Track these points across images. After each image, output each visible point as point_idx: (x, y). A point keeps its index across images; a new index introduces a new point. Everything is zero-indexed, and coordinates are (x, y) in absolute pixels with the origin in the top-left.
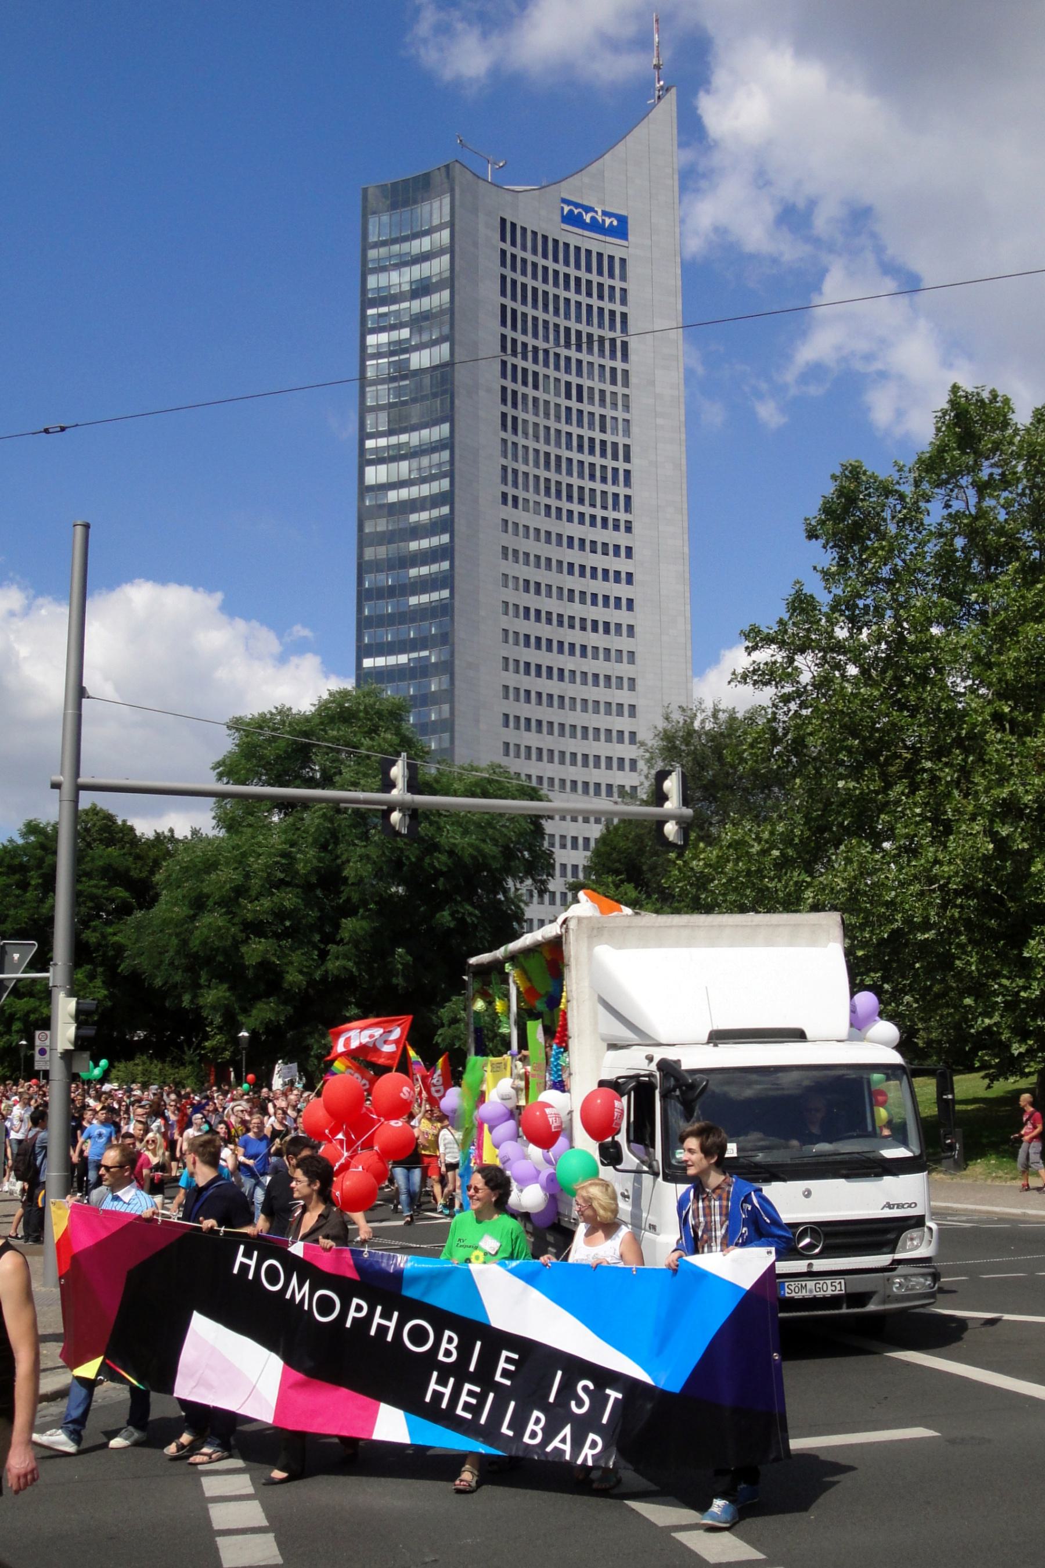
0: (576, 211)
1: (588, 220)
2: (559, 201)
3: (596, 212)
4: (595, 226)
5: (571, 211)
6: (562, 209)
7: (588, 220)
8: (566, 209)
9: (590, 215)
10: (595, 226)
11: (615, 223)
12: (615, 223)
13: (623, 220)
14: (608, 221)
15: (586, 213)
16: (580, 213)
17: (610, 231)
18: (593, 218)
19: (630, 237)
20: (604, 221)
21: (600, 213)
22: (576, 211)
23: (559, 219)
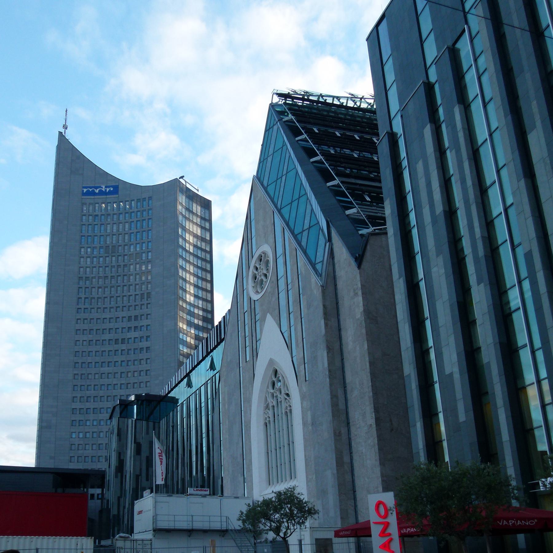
0: (91, 190)
1: (97, 191)
4: (101, 193)
6: (83, 191)
7: (97, 191)
8: (85, 190)
9: (98, 190)
10: (101, 193)
11: (112, 189)
12: (112, 189)
14: (108, 190)
15: (96, 189)
17: (110, 193)
19: (119, 193)
20: (106, 190)
21: (104, 187)
22: (91, 190)
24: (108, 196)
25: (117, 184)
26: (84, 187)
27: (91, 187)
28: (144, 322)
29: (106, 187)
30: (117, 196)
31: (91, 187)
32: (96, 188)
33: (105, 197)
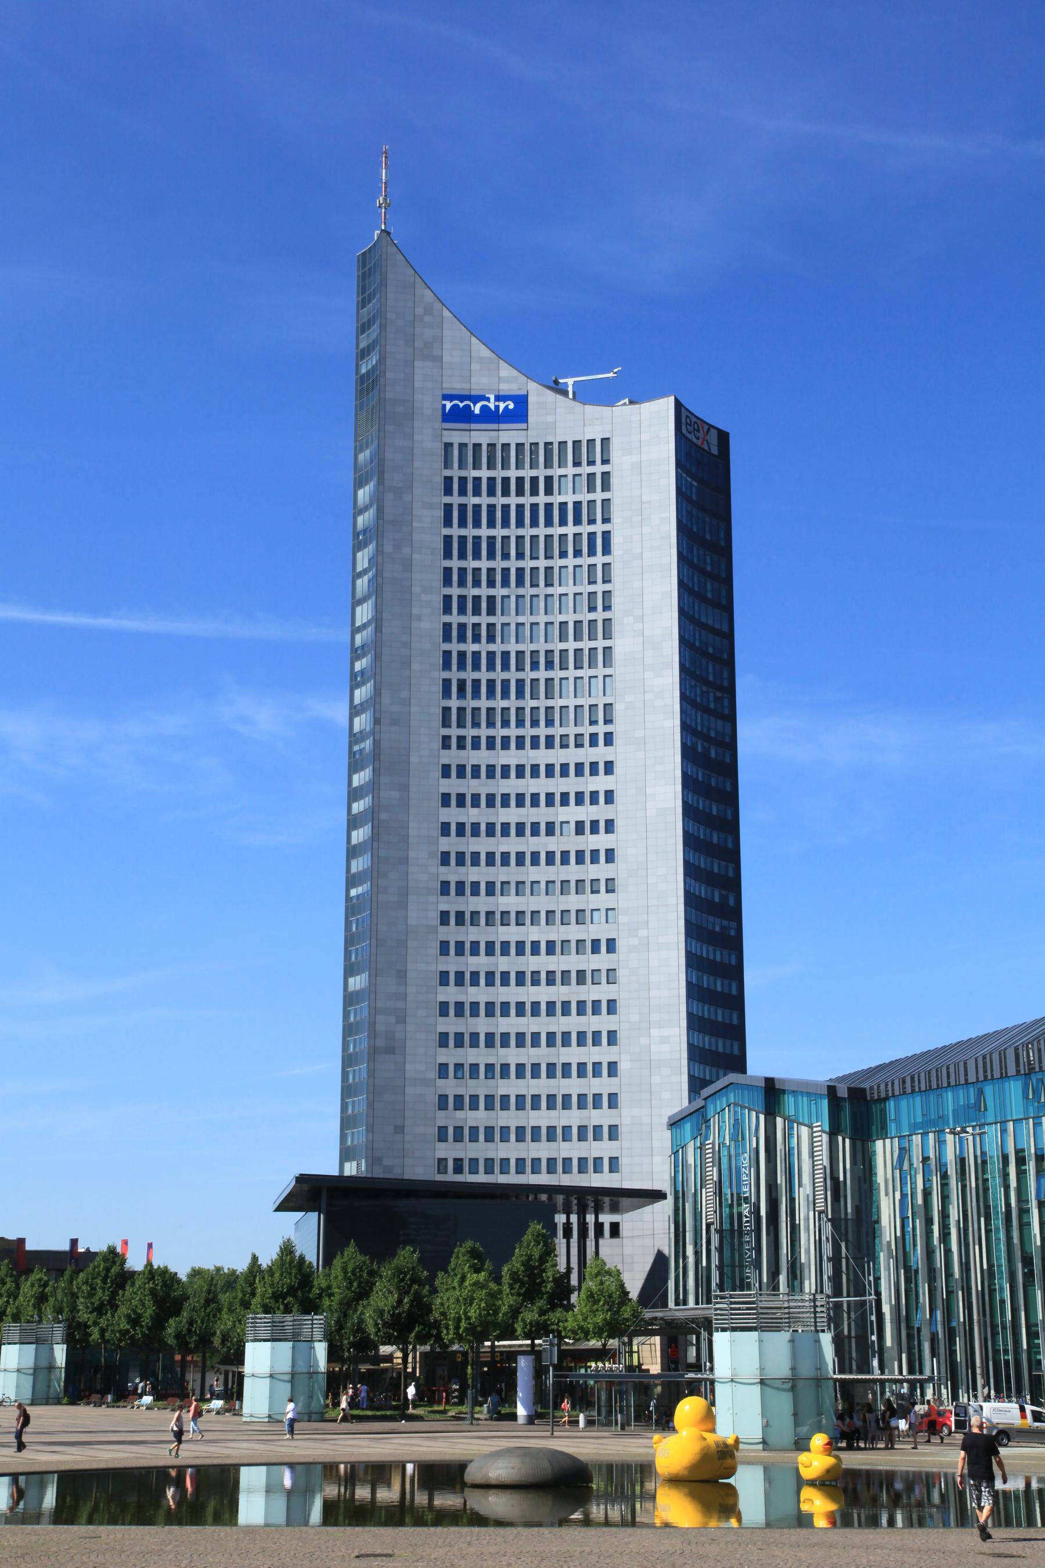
0: (461, 405)
1: (477, 411)
2: (440, 398)
3: (488, 399)
5: (455, 406)
6: (444, 406)
7: (477, 411)
8: (449, 405)
11: (511, 406)
12: (511, 406)
13: (521, 401)
14: (502, 406)
16: (468, 407)
18: (484, 408)
19: (531, 418)
20: (497, 407)
21: (492, 398)
22: (461, 405)
23: (440, 418)
24: (502, 426)
25: (523, 392)
26: (446, 397)
27: (461, 398)
28: (600, 783)
29: (498, 398)
30: (524, 426)
31: (461, 398)
32: (475, 399)
33: (495, 426)
